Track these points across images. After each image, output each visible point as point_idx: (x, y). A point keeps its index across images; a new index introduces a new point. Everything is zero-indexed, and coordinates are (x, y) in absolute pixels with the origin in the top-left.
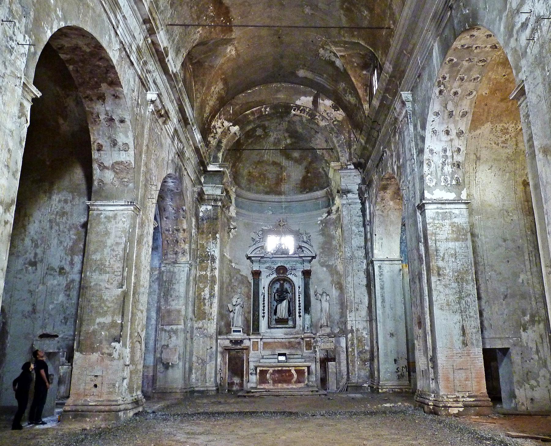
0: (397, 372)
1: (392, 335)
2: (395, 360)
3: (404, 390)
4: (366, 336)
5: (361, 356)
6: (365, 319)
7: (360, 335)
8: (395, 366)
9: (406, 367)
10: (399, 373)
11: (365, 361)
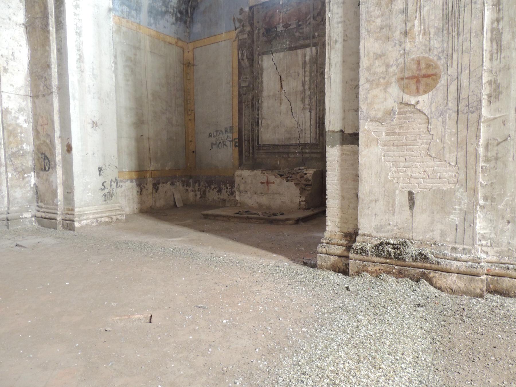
0: (102, 189)
1: (95, 124)
2: (100, 170)
3: (114, 218)
4: (25, 125)
5: (17, 162)
6: (22, 92)
7: (13, 122)
8: (101, 180)
9: (116, 179)
10: (106, 191)
11: (24, 171)
